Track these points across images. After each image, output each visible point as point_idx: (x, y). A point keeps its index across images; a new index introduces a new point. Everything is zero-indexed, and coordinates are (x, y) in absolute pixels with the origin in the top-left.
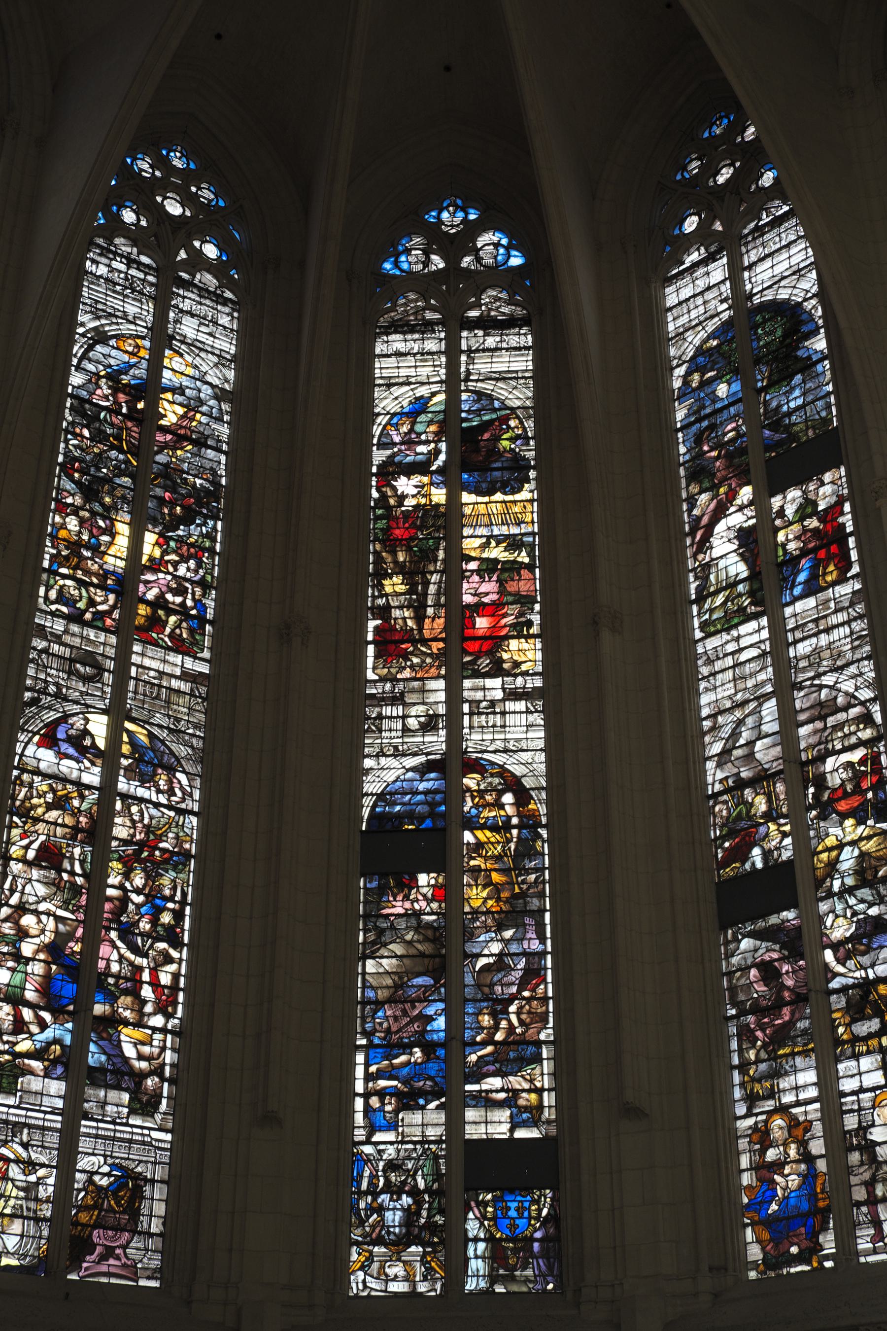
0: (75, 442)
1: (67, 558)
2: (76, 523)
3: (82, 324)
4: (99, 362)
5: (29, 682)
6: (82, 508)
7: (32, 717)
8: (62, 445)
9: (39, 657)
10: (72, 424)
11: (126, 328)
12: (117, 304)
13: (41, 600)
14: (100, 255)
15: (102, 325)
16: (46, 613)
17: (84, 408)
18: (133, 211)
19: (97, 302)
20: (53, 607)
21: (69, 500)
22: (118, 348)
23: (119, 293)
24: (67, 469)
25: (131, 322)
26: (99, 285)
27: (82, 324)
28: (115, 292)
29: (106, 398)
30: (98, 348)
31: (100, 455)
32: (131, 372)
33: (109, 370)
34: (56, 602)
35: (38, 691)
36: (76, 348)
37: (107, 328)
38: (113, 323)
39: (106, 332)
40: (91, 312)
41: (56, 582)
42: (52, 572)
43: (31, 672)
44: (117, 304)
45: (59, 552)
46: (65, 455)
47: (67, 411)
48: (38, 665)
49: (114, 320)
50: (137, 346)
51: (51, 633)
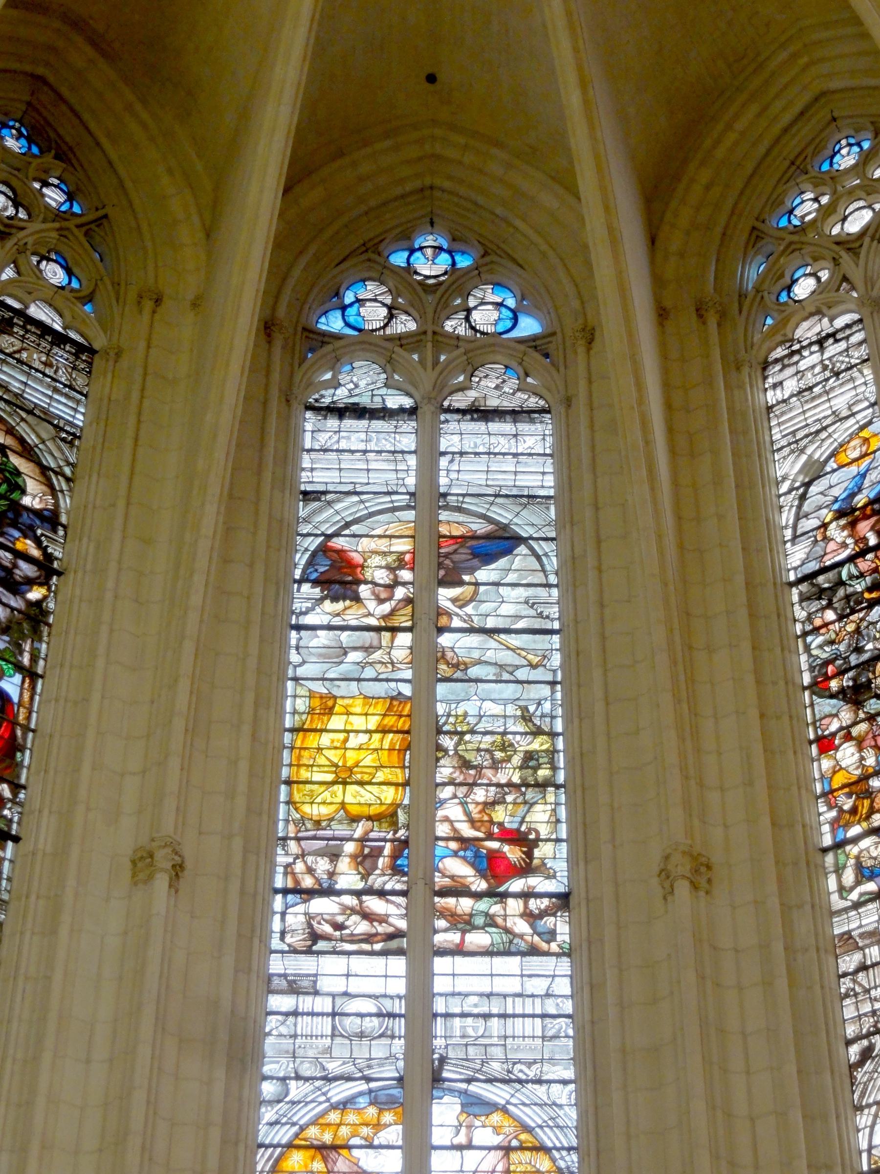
0: (820, 640)
1: (854, 811)
2: (853, 750)
3: (784, 478)
4: (820, 508)
5: (851, 1031)
6: (855, 723)
7: (869, 1080)
8: (804, 658)
9: (854, 981)
10: (809, 619)
11: (841, 431)
12: (821, 410)
13: (835, 897)
14: (781, 370)
15: (810, 456)
16: (846, 910)
17: (820, 585)
18: (810, 275)
19: (794, 433)
20: (854, 896)
21: (834, 726)
22: (841, 467)
23: (820, 396)
24: (819, 687)
25: (847, 418)
26: (791, 410)
27: (784, 478)
28: (813, 399)
29: (844, 545)
30: (813, 489)
31: (858, 631)
32: (867, 483)
33: (836, 506)
34: (858, 883)
35: (869, 1035)
36: (784, 516)
37: (816, 456)
38: (823, 440)
39: (818, 460)
40: (792, 452)
41: (847, 856)
42: (839, 845)
43: (849, 1012)
44: (821, 410)
45: (841, 811)
46: (812, 669)
47: (797, 607)
48: (856, 995)
49: (824, 435)
50: (866, 441)
51: (861, 936)
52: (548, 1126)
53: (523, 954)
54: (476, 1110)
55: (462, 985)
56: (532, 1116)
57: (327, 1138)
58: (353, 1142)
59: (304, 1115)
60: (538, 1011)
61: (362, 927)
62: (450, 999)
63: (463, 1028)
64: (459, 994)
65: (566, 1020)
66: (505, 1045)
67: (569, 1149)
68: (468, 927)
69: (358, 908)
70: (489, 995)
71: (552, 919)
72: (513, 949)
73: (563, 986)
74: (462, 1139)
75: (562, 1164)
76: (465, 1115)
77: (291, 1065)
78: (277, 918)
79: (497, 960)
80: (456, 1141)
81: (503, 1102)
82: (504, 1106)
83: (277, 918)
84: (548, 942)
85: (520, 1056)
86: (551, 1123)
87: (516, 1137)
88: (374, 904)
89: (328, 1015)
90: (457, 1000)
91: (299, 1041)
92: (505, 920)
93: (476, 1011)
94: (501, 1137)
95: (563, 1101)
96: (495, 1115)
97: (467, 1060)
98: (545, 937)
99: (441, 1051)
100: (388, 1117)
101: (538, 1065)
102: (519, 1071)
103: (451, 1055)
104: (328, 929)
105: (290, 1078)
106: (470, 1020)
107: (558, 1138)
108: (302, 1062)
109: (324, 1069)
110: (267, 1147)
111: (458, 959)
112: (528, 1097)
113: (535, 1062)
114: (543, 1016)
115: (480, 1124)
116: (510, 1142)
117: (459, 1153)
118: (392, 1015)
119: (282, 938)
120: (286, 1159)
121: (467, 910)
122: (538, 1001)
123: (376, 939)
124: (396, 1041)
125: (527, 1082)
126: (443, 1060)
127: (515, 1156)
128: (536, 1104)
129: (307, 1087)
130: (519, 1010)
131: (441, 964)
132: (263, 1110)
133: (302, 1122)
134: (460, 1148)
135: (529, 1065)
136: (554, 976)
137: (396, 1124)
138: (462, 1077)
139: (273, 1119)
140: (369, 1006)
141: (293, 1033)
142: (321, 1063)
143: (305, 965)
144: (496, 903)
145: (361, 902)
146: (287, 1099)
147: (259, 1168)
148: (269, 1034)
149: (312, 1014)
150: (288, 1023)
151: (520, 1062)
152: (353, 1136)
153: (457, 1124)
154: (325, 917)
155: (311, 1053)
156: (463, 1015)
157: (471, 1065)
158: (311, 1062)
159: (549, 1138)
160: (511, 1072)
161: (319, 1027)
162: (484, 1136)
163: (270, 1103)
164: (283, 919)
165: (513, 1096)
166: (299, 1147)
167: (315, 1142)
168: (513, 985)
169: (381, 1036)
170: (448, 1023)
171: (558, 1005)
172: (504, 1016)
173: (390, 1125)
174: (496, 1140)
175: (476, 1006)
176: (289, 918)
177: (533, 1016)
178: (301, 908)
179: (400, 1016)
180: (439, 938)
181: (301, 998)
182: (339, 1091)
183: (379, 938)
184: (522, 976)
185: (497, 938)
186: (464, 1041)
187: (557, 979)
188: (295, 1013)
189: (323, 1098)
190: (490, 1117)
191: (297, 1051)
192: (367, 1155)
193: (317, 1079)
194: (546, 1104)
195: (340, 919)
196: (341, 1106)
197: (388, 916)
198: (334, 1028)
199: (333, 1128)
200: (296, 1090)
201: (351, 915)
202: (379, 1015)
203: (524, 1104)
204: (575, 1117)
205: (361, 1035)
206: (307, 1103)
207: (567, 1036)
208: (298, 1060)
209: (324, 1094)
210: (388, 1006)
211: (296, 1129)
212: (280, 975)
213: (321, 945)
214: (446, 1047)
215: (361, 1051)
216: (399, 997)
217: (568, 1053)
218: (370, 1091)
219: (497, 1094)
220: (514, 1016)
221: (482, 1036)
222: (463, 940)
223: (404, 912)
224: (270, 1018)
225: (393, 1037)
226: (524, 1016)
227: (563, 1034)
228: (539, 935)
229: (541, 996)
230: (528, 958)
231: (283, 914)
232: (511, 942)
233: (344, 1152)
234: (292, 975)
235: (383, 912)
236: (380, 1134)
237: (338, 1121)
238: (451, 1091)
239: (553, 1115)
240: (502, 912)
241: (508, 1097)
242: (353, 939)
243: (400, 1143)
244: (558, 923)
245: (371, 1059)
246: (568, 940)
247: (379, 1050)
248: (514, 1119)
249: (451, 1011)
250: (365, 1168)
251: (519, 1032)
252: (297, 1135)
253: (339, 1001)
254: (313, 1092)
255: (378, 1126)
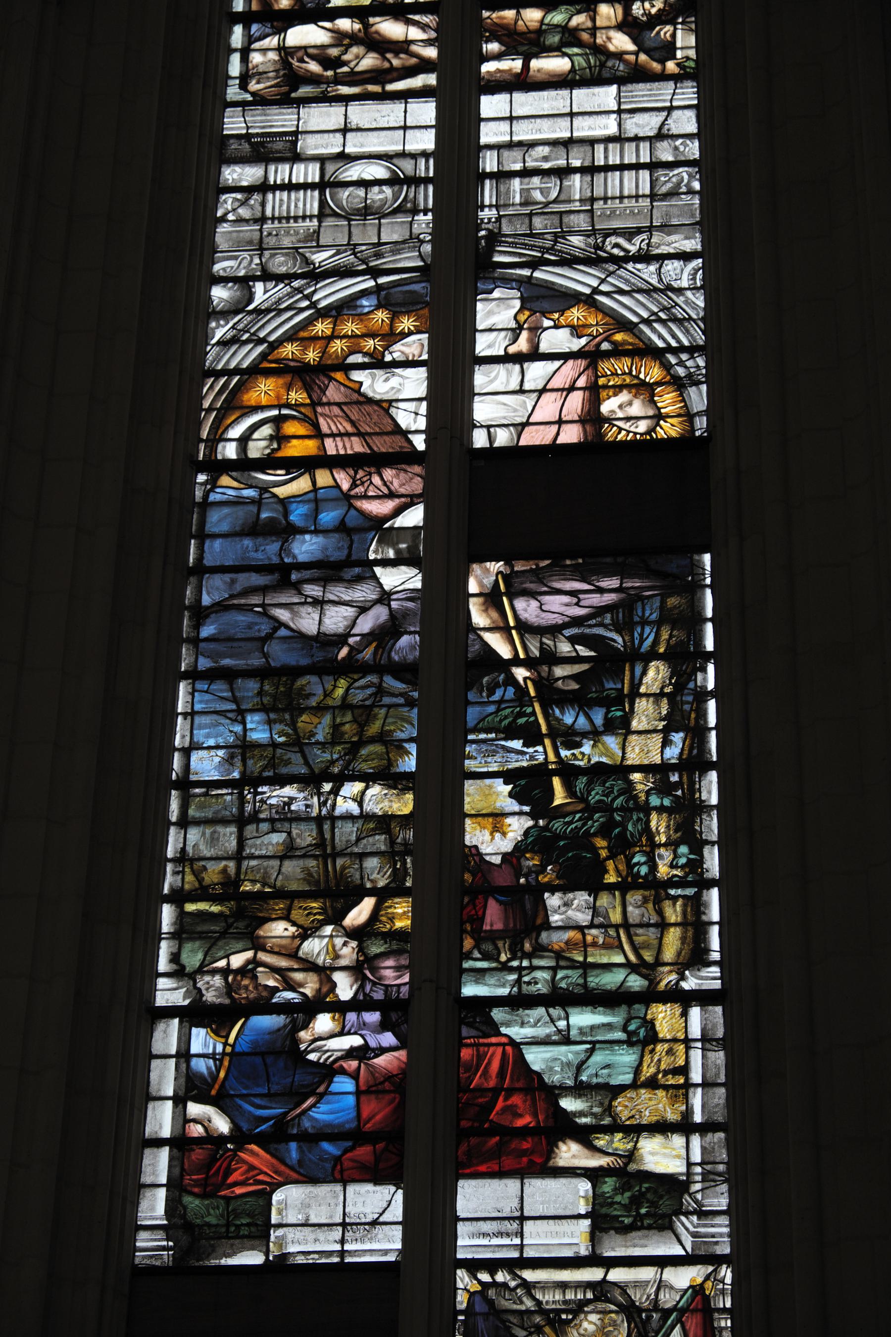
52: (660, 320)
53: (621, 81)
54: (546, 305)
55: (524, 132)
56: (633, 308)
57: (312, 356)
58: (352, 359)
59: (274, 328)
60: (645, 158)
61: (369, 61)
62: (505, 153)
63: (525, 192)
64: (520, 144)
65: (690, 170)
66: (591, 211)
67: (692, 350)
68: (535, 50)
69: (362, 34)
70: (568, 143)
71: (669, 28)
72: (606, 74)
73: (686, 122)
74: (522, 344)
75: (681, 371)
76: (527, 313)
77: (257, 261)
78: (236, 58)
79: (579, 94)
80: (512, 350)
81: (587, 291)
82: (590, 296)
83: (236, 58)
84: (662, 62)
85: (616, 224)
86: (662, 315)
87: (606, 339)
88: (391, 29)
89: (312, 186)
90: (517, 154)
91: (268, 226)
92: (594, 35)
93: (546, 166)
94: (583, 341)
95: (685, 283)
96: (574, 310)
97: (531, 235)
98: (657, 55)
99: (490, 226)
100: (406, 323)
101: (644, 236)
102: (613, 245)
103: (506, 229)
104: (314, 67)
105: (256, 279)
106: (536, 181)
107: (674, 336)
108: (273, 256)
109: (307, 262)
110: (218, 374)
111: (518, 96)
112: (627, 281)
113: (639, 231)
114: (653, 166)
115: (551, 323)
116: (600, 344)
117: (517, 367)
118: (414, 181)
119: (243, 86)
120: (248, 391)
121: (534, 25)
122: (645, 147)
123: (389, 77)
124: (421, 217)
125: (627, 258)
126: (494, 238)
127: (605, 366)
128: (640, 291)
129: (281, 289)
130: (614, 159)
131: (491, 105)
132: (213, 324)
133: (272, 338)
134: (519, 359)
135: (630, 234)
136: (670, 109)
137: (419, 332)
138: (524, 259)
139: (228, 336)
140: (378, 171)
141: (259, 215)
142: (303, 255)
143: (281, 120)
144: (579, 12)
145: (367, 26)
146: (251, 307)
147: (206, 404)
148: (223, 219)
149: (290, 187)
150: (252, 202)
151: (615, 232)
152: (352, 353)
153: (513, 325)
154: (310, 51)
155: (287, 242)
156: (526, 173)
157: (539, 242)
158: (283, 255)
159: (661, 337)
160: (602, 249)
161: (301, 205)
162: (556, 339)
163: (225, 314)
164: (245, 59)
165: (603, 281)
166: (268, 373)
167: (292, 364)
168: (609, 125)
169: (395, 212)
170: (502, 188)
171: (676, 148)
172: (590, 170)
173: (410, 333)
174: (577, 344)
175: (546, 159)
176: (256, 58)
177: (637, 167)
178: (272, 41)
179: (426, 181)
180: (488, 67)
181: (272, 168)
182: (329, 293)
183: (395, 74)
184: (619, 112)
185: (580, 61)
186: (526, 210)
187: (676, 114)
188: (264, 187)
189: (306, 303)
190: (568, 313)
191: (266, 240)
192: (373, 377)
193: (296, 276)
194: (656, 290)
195: (334, 52)
196: (334, 313)
197: (409, 42)
198: (323, 203)
199: (320, 344)
200: (261, 293)
201: (350, 46)
202: (393, 181)
203: (621, 292)
204: (702, 305)
205: (366, 211)
206: (280, 312)
207: (691, 192)
208: (267, 254)
209: (308, 297)
210: (407, 166)
211: (260, 349)
212: (238, 137)
213: (304, 91)
214: (499, 218)
215: (365, 234)
216: (425, 154)
217: (693, 216)
218: (379, 288)
219: (581, 280)
220: (607, 168)
221: (555, 201)
222: (526, 66)
223: (433, 35)
224: (223, 197)
225: (415, 211)
226: (622, 168)
227: (684, 189)
228: (647, 53)
229: (649, 139)
230: (630, 87)
231: (245, 53)
232: (602, 65)
233: (339, 376)
234: (257, 135)
235: (402, 38)
236: (397, 347)
237: (328, 332)
238: (507, 282)
239: (665, 302)
240: (589, 24)
241: (595, 283)
242: (354, 78)
243: (425, 357)
244: (679, 33)
245: (379, 244)
246: (692, 53)
247: (392, 231)
248: (605, 314)
249: (506, 168)
250: (371, 394)
251: (613, 190)
252: (263, 356)
253: (330, 168)
254: (290, 295)
255: (392, 337)
